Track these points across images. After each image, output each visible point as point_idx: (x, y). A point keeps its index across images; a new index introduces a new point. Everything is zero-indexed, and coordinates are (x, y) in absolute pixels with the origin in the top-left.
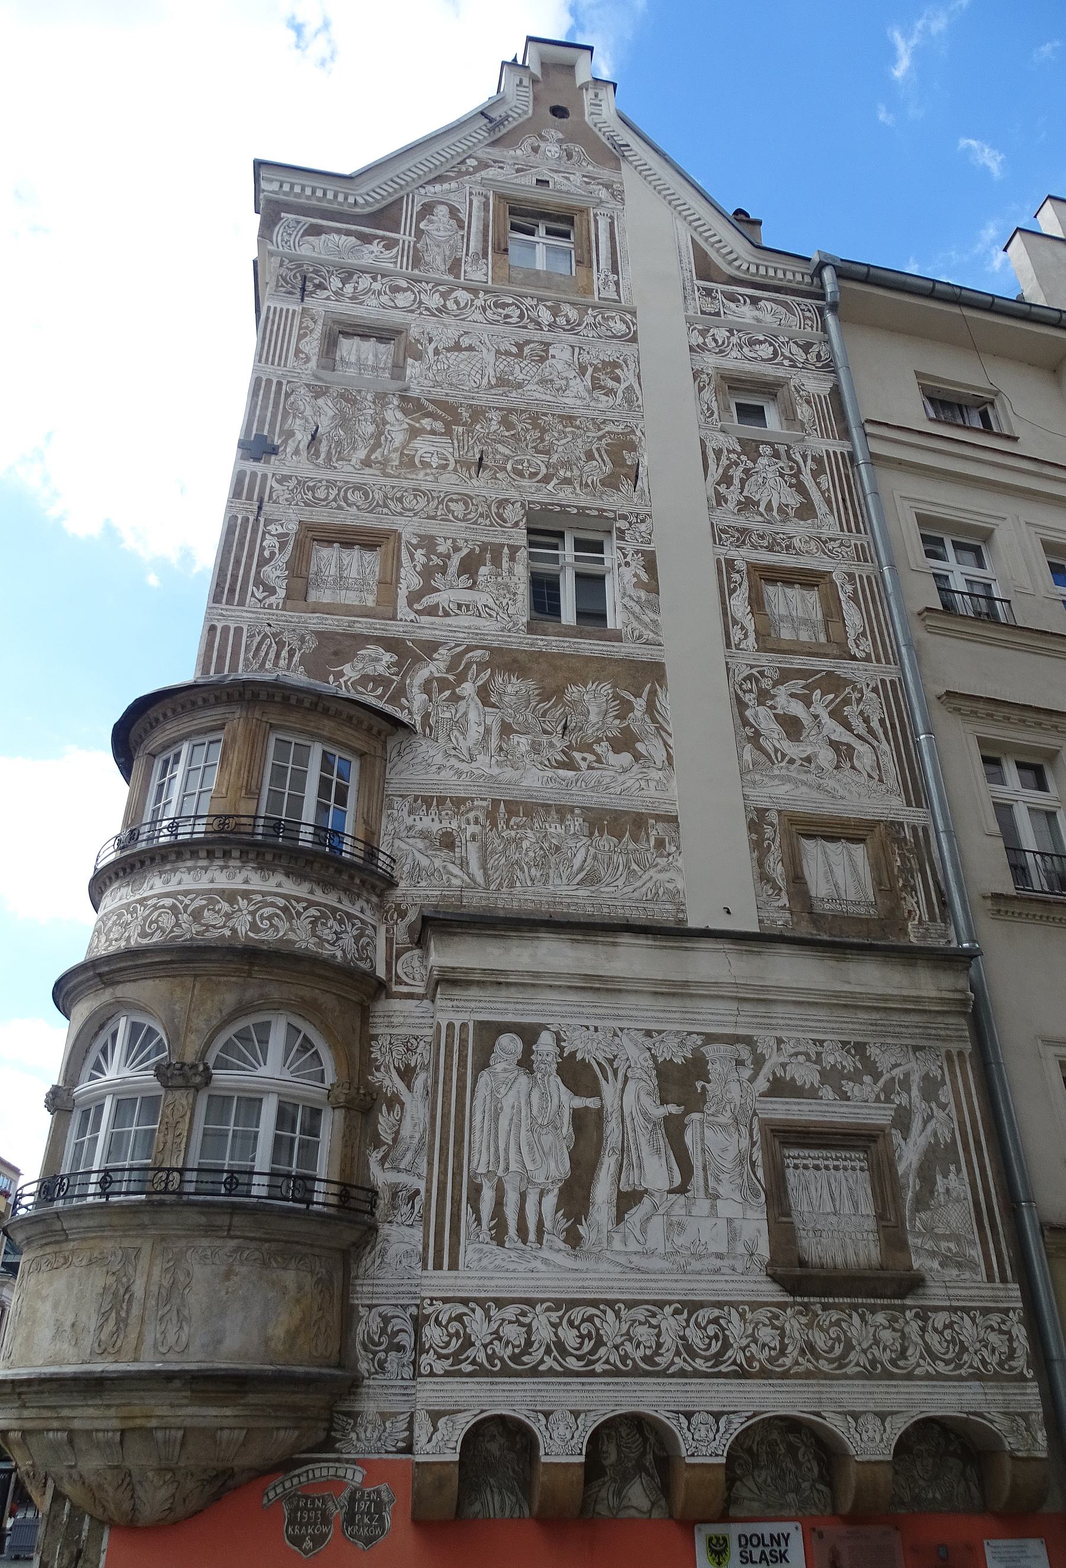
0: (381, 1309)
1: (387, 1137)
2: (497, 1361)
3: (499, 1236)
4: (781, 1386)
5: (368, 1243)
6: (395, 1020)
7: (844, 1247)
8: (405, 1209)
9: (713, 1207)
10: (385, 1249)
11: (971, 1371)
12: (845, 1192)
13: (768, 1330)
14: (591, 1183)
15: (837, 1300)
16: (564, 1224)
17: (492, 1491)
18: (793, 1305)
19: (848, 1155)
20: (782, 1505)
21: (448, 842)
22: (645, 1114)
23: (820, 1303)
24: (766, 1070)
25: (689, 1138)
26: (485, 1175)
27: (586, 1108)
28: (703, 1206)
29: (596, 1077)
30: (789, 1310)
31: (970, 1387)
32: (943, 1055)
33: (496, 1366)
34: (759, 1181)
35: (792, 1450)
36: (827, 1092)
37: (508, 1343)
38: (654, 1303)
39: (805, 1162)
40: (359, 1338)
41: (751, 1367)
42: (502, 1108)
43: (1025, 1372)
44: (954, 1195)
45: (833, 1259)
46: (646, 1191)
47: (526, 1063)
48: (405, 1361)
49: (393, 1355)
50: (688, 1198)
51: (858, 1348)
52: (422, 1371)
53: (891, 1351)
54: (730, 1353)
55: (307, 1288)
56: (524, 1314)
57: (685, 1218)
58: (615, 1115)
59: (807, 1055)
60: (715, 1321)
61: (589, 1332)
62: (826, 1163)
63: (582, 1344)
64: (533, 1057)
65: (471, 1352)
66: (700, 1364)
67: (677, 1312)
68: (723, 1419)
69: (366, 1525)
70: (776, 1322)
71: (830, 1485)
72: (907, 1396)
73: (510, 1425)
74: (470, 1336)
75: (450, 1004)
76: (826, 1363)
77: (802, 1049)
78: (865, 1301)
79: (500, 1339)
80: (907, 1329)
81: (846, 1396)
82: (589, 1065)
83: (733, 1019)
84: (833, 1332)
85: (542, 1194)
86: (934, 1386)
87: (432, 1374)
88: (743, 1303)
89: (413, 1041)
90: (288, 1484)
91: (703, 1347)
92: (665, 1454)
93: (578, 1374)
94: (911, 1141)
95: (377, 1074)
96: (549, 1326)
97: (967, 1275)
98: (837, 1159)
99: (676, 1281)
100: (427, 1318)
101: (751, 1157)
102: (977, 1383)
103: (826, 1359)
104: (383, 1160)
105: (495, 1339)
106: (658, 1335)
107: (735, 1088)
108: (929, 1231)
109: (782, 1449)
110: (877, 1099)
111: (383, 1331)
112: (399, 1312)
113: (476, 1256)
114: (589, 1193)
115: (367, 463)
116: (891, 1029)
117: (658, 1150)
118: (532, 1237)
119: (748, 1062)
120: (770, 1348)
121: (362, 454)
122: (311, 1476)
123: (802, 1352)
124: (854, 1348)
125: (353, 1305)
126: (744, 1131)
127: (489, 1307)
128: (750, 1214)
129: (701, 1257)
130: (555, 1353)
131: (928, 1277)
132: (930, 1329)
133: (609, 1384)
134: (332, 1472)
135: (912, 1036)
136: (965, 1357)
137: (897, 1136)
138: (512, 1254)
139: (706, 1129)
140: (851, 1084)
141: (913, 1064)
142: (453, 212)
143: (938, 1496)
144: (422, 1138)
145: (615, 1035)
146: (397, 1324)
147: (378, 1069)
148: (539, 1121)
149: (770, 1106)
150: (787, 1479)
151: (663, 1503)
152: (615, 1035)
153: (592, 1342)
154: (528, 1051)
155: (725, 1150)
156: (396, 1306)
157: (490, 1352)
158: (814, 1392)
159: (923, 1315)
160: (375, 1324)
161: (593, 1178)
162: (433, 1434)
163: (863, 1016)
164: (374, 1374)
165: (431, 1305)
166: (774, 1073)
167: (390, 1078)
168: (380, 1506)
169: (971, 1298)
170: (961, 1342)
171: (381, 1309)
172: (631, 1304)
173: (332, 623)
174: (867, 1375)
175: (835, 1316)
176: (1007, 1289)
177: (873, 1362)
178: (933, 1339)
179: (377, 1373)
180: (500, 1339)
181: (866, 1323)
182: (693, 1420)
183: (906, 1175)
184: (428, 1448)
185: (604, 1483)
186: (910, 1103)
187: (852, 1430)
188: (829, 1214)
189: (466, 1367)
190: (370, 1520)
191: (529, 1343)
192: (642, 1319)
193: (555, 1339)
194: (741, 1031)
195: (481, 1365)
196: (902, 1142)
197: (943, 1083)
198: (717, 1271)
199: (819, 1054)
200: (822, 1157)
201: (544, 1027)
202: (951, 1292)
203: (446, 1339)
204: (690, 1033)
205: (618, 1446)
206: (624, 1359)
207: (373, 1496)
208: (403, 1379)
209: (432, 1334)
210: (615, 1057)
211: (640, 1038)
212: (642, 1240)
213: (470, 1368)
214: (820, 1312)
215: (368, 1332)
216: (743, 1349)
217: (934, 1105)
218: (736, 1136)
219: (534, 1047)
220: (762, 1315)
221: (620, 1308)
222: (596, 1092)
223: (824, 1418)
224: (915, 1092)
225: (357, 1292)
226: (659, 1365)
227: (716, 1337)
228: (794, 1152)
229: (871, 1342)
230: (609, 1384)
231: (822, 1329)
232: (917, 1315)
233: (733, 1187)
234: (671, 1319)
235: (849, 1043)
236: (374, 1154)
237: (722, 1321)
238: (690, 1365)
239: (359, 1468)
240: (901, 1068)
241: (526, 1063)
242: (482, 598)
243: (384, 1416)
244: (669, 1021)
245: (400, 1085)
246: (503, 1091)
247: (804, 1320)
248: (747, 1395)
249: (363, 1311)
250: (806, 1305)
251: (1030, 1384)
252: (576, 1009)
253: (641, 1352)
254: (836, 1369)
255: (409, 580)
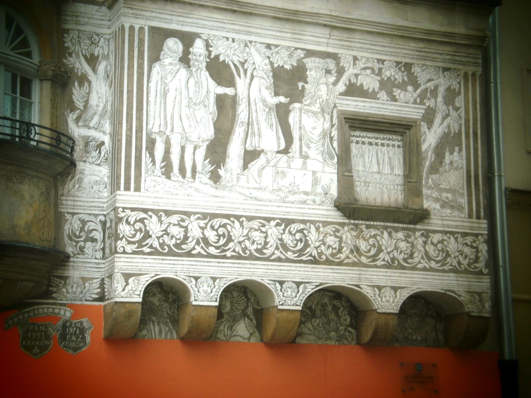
0: (80, 216)
1: (80, 105)
2: (165, 247)
3: (167, 171)
4: (337, 269)
5: (69, 174)
6: (82, 20)
7: (382, 193)
8: (95, 154)
9: (304, 163)
10: (81, 178)
11: (451, 267)
12: (386, 159)
13: (332, 238)
14: (227, 143)
15: (375, 223)
16: (209, 168)
17: (154, 324)
18: (349, 224)
19: (391, 137)
20: (327, 338)
22: (264, 101)
23: (365, 224)
24: (344, 78)
25: (293, 119)
26: (158, 133)
27: (226, 95)
28: (298, 162)
29: (232, 74)
30: (346, 228)
31: (449, 276)
32: (462, 74)
33: (165, 249)
34: (334, 149)
35: (336, 309)
36: (383, 95)
37: (172, 237)
38: (265, 219)
39: (363, 140)
40: (66, 232)
41: (320, 258)
42: (168, 90)
43: (483, 270)
44: (455, 165)
45: (375, 200)
46: (262, 151)
48: (97, 248)
49: (89, 244)
50: (289, 157)
51: (385, 251)
52: (118, 250)
53: (405, 254)
54: (308, 250)
55: (36, 198)
56: (183, 220)
57: (286, 169)
58: (244, 100)
59: (372, 69)
60: (301, 231)
61: (224, 233)
62: (377, 141)
63: (219, 240)
64: (190, 56)
65: (149, 241)
66: (290, 255)
67: (278, 225)
68: (301, 287)
69: (74, 341)
70: (337, 234)
71: (356, 329)
72: (411, 279)
73: (165, 288)
74: (149, 231)
75: (131, 11)
76: (365, 258)
77: (369, 65)
78: (392, 225)
79: (168, 234)
80: (415, 243)
81: (376, 277)
82: (228, 66)
83: (325, 40)
84: (371, 241)
85: (195, 148)
86: (428, 275)
87: (124, 252)
88: (318, 221)
89: (95, 37)
90: (21, 317)
91: (293, 245)
92: (260, 308)
93: (215, 257)
94: (433, 130)
95: (70, 59)
96: (199, 229)
97: (456, 213)
98: (384, 139)
99: (279, 206)
100: (120, 220)
101: (330, 134)
102: (453, 274)
103: (365, 256)
104: (77, 120)
105: (164, 234)
106: (266, 237)
107: (323, 89)
108: (437, 186)
109: (330, 308)
110: (415, 102)
111: (82, 229)
112: (92, 218)
113: (153, 184)
114: (226, 150)
116: (430, 55)
117: (271, 125)
118: (189, 174)
119: (333, 72)
120: (333, 249)
122: (36, 312)
123: (352, 251)
124: (382, 251)
125: (61, 212)
126: (328, 117)
127: (161, 215)
128: (327, 169)
129: (295, 193)
130: (202, 244)
131: (432, 213)
132: (429, 242)
133: (234, 263)
134: (50, 310)
135: (444, 61)
136: (449, 260)
137: (424, 127)
138: (176, 184)
139: (303, 114)
140: (399, 91)
141: (441, 80)
143: (419, 338)
144: (105, 107)
145: (246, 45)
146: (91, 226)
147: (70, 55)
148: (194, 101)
149: (345, 102)
150: (331, 325)
151: (257, 334)
152: (246, 45)
153: (225, 239)
154: (186, 52)
155: (314, 128)
156: (90, 214)
157: (161, 241)
158: (356, 274)
159: (426, 234)
160: (77, 225)
161: (229, 140)
162: (125, 286)
163: (413, 44)
164: (77, 254)
165: (123, 212)
166: (350, 80)
167: (80, 62)
168: (82, 331)
169: (457, 227)
170: (447, 251)
171: (80, 216)
172: (250, 219)
174: (388, 266)
175: (373, 232)
176: (479, 223)
177: (393, 259)
178: (430, 249)
179: (78, 254)
180: (168, 234)
181: (392, 237)
182: (284, 286)
183: (427, 151)
184: (123, 294)
185: (222, 322)
186: (436, 106)
187: (377, 296)
188: (375, 173)
189: (146, 250)
190: (77, 338)
191: (186, 238)
192: (257, 227)
193: (202, 236)
194: (331, 50)
195: (156, 249)
196: (427, 131)
197: (459, 93)
198: (304, 202)
199: (380, 69)
200: (375, 138)
201: (197, 35)
202: (445, 222)
203: (133, 232)
204: (296, 49)
205: (232, 303)
206: (244, 249)
207: (78, 325)
208: (96, 258)
209: (124, 229)
210: (246, 61)
211: (264, 50)
212: (259, 181)
213: (149, 250)
214: (364, 230)
215: (72, 229)
216: (317, 248)
217: (451, 108)
218: (322, 119)
219: (191, 49)
220: (330, 229)
221: (243, 221)
222: (231, 83)
223: (361, 288)
224: (440, 99)
225: (63, 205)
226: (265, 254)
227: (301, 240)
228: (357, 133)
229: (393, 248)
230: (234, 263)
231: (364, 239)
232: (422, 235)
233: (318, 152)
234: (274, 229)
235: (401, 63)
236: (71, 115)
237: (305, 232)
238: (284, 255)
239: (68, 309)
240: (433, 82)
243: (84, 280)
244: (283, 39)
245: (87, 69)
246: (169, 78)
247: (354, 233)
248: (317, 274)
249: (68, 216)
250: (356, 225)
251: (485, 277)
252: (220, 25)
253: (255, 246)
254: (370, 262)
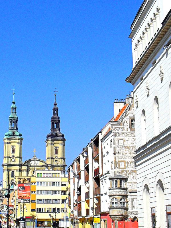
21: (130, 186)
47: (136, 200)
115: (123, 154)
121: (122, 153)
142: (126, 122)
173: (122, 170)
241: (136, 200)
242: (131, 166)
255: (127, 165)
